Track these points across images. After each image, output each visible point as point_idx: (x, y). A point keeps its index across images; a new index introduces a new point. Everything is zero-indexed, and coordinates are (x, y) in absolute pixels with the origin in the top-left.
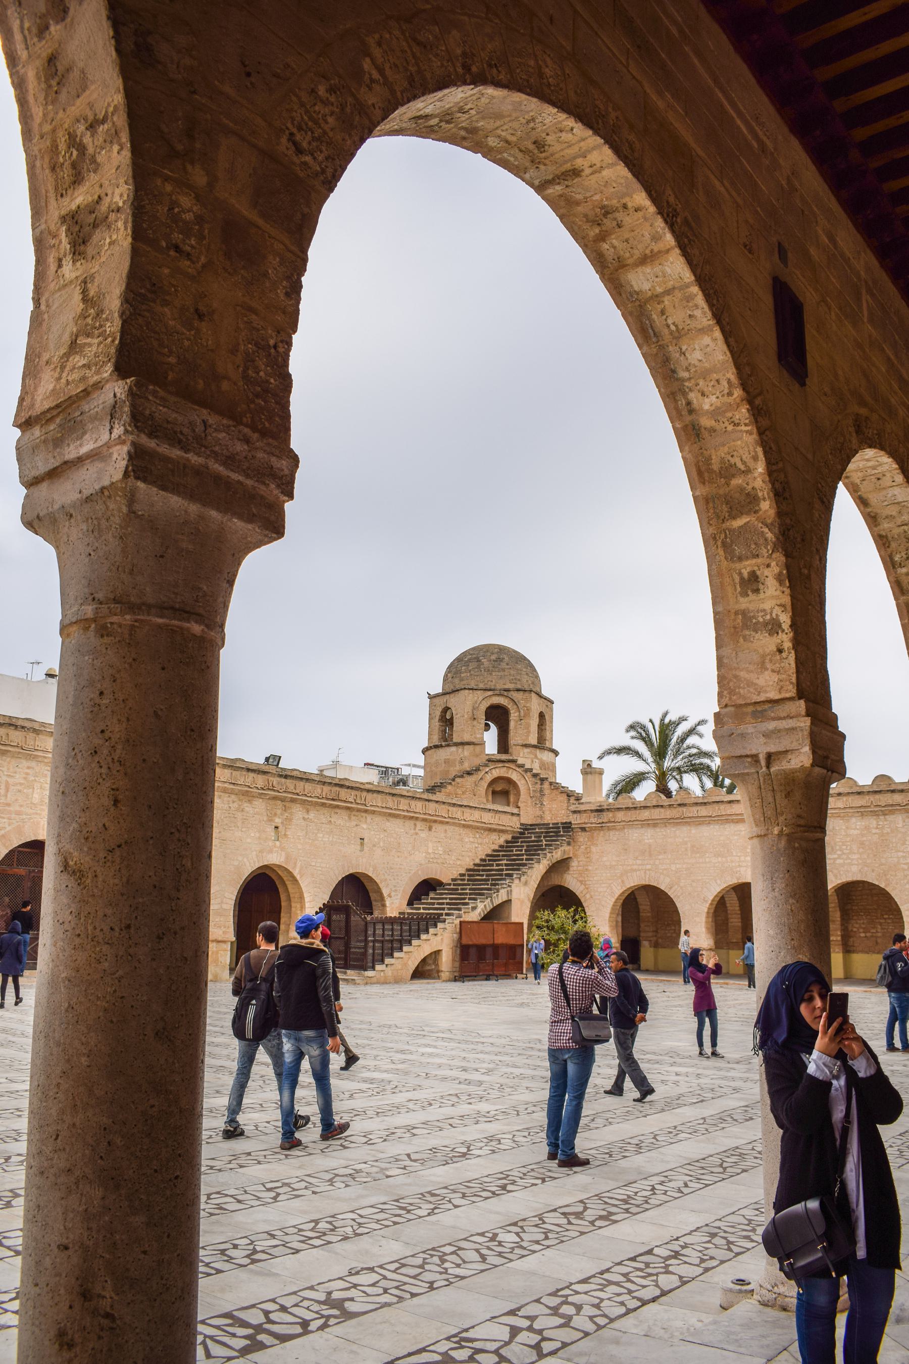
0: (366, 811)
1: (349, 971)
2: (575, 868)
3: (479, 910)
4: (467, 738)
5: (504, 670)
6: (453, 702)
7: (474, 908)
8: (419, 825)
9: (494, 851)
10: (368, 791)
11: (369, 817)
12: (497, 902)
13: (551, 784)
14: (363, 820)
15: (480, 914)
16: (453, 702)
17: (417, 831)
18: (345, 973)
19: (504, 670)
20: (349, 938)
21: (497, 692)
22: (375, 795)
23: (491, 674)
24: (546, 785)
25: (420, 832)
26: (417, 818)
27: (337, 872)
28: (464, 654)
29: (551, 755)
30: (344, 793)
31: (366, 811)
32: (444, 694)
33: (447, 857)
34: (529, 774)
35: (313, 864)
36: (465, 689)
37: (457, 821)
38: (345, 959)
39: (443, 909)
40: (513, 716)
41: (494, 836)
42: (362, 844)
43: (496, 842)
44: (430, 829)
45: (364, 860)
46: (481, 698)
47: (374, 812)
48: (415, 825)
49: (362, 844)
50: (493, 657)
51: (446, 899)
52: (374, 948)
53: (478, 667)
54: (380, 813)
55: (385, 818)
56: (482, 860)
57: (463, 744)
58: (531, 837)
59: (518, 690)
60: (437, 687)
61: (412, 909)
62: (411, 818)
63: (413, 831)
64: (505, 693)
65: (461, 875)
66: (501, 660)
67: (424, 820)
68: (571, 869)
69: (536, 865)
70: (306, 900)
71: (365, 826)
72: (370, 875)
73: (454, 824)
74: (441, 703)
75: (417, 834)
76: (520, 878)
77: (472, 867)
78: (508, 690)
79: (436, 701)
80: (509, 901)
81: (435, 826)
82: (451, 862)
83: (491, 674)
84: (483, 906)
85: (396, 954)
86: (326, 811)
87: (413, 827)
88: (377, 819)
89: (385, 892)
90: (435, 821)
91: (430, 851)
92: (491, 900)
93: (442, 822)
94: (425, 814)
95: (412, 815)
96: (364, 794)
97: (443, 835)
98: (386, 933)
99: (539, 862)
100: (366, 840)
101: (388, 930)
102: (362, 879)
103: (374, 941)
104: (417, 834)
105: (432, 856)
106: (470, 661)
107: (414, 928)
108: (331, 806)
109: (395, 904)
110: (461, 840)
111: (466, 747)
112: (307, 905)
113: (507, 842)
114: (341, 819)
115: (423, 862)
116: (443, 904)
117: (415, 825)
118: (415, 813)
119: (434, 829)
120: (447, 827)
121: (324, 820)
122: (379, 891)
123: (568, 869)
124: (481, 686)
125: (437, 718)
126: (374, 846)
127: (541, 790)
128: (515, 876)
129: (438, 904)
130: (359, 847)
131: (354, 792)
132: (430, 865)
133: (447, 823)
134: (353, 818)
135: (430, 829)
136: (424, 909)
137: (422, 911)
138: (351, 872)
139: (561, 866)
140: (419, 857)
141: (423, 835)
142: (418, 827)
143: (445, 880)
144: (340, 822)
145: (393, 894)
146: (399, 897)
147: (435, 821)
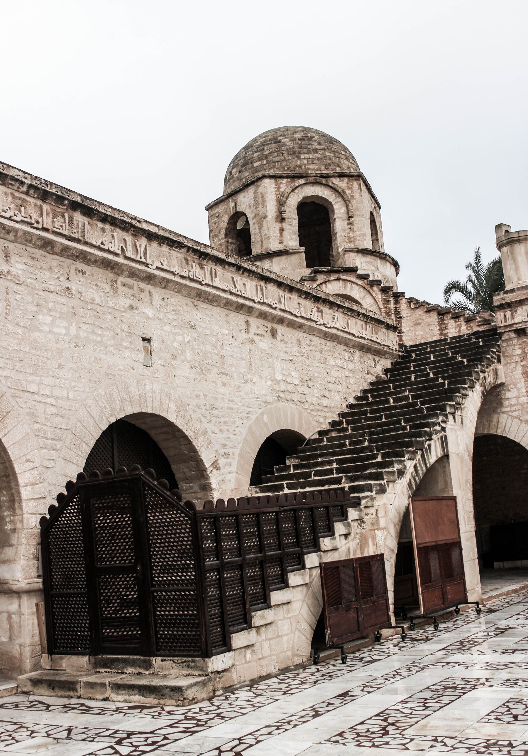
0: (150, 278)
1: (157, 661)
2: (513, 401)
3: (408, 476)
4: (275, 246)
5: (315, 151)
6: (245, 202)
7: (401, 473)
8: (254, 322)
9: (372, 384)
10: (151, 236)
11: (158, 293)
12: (432, 459)
13: (410, 300)
14: (145, 296)
15: (410, 485)
16: (245, 202)
17: (252, 335)
18: (148, 666)
19: (315, 151)
20: (148, 567)
21: (311, 179)
22: (165, 248)
23: (299, 158)
24: (403, 305)
25: (256, 338)
26: (250, 310)
27: (95, 411)
28: (255, 140)
29: (393, 268)
30: (96, 234)
31: (150, 278)
32: (231, 195)
33: (306, 390)
34: (375, 288)
35: (33, 388)
36: (264, 177)
37: (313, 325)
38: (143, 622)
39: (338, 481)
40: (339, 210)
41: (369, 359)
42: (149, 352)
43: (372, 371)
44: (274, 334)
45: (157, 387)
46: (289, 189)
47: (165, 284)
48: (247, 322)
49: (149, 352)
50: (297, 136)
51: (330, 463)
52: (220, 584)
53: (278, 151)
54: (180, 289)
55: (189, 301)
56: (357, 398)
57: (270, 255)
58: (430, 358)
59: (341, 176)
60: (219, 192)
61: (263, 490)
62: (240, 308)
63: (244, 336)
64: (324, 181)
65: (334, 424)
66: (311, 139)
67: (263, 315)
68: (506, 403)
69: (469, 393)
70: (22, 479)
71: (150, 312)
72: (172, 418)
73: (311, 331)
74: (224, 213)
75: (252, 341)
76: (453, 414)
77: (346, 410)
78: (327, 177)
79: (219, 210)
80: (446, 457)
81: (281, 329)
82: (315, 401)
83: (299, 158)
84: (412, 469)
85: (276, 597)
86: (54, 261)
87: (244, 327)
88: (176, 300)
89: (206, 457)
90: (281, 321)
91: (279, 377)
92: (422, 455)
93: (291, 324)
94: (263, 304)
95: (241, 301)
96: (143, 242)
97: (295, 349)
98: (246, 544)
99: (472, 387)
100: (155, 344)
101: (229, 538)
102: (153, 433)
103: (220, 569)
104: (252, 341)
105: (283, 388)
106: (264, 144)
107: (305, 525)
108: (65, 251)
109: (229, 480)
110: (324, 361)
111: (275, 260)
112: (25, 493)
113: (386, 371)
114: (92, 286)
115: (269, 398)
116: (330, 471)
117: (247, 322)
118: (245, 298)
119: (279, 336)
120: (301, 335)
121: (52, 284)
122: (192, 456)
123: (501, 404)
124: (286, 173)
125: (223, 232)
126: (174, 357)
127: (397, 312)
128: (448, 410)
129: (317, 473)
130: (141, 357)
131: (118, 234)
132: (280, 405)
133: (301, 326)
134: (121, 289)
135: (274, 334)
136: (290, 487)
137: (287, 491)
138: (130, 411)
139: (493, 398)
140: (262, 387)
141: (265, 343)
142: (253, 330)
143: (309, 432)
144: (90, 293)
145: (221, 462)
146: (234, 468)
147: (281, 321)
